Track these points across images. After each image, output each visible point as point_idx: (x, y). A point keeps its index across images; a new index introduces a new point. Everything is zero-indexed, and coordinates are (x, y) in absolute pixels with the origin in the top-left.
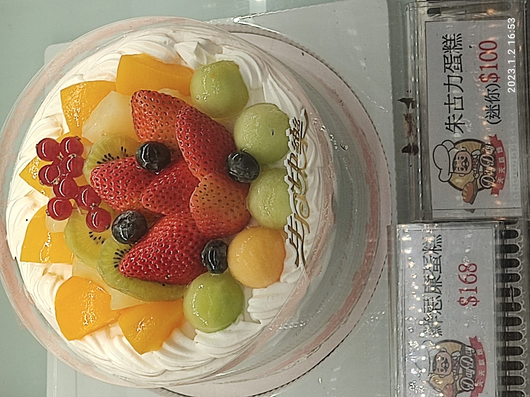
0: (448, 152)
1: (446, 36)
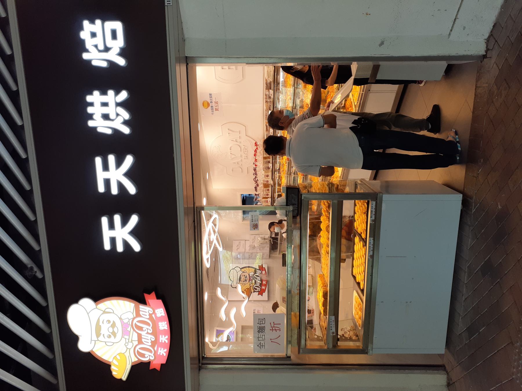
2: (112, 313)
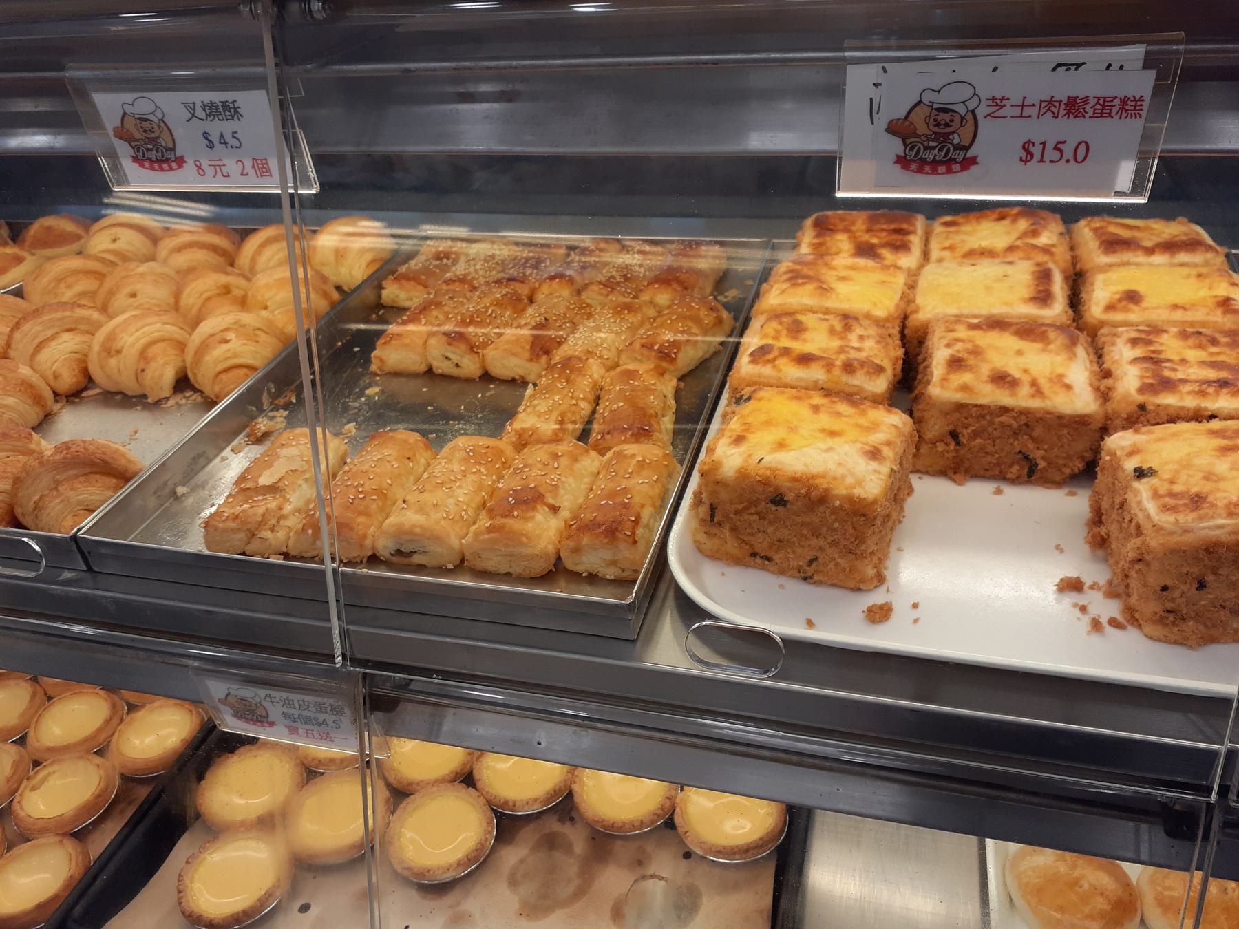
0: (963, 102)
1: (1143, 100)
2: (961, 123)
